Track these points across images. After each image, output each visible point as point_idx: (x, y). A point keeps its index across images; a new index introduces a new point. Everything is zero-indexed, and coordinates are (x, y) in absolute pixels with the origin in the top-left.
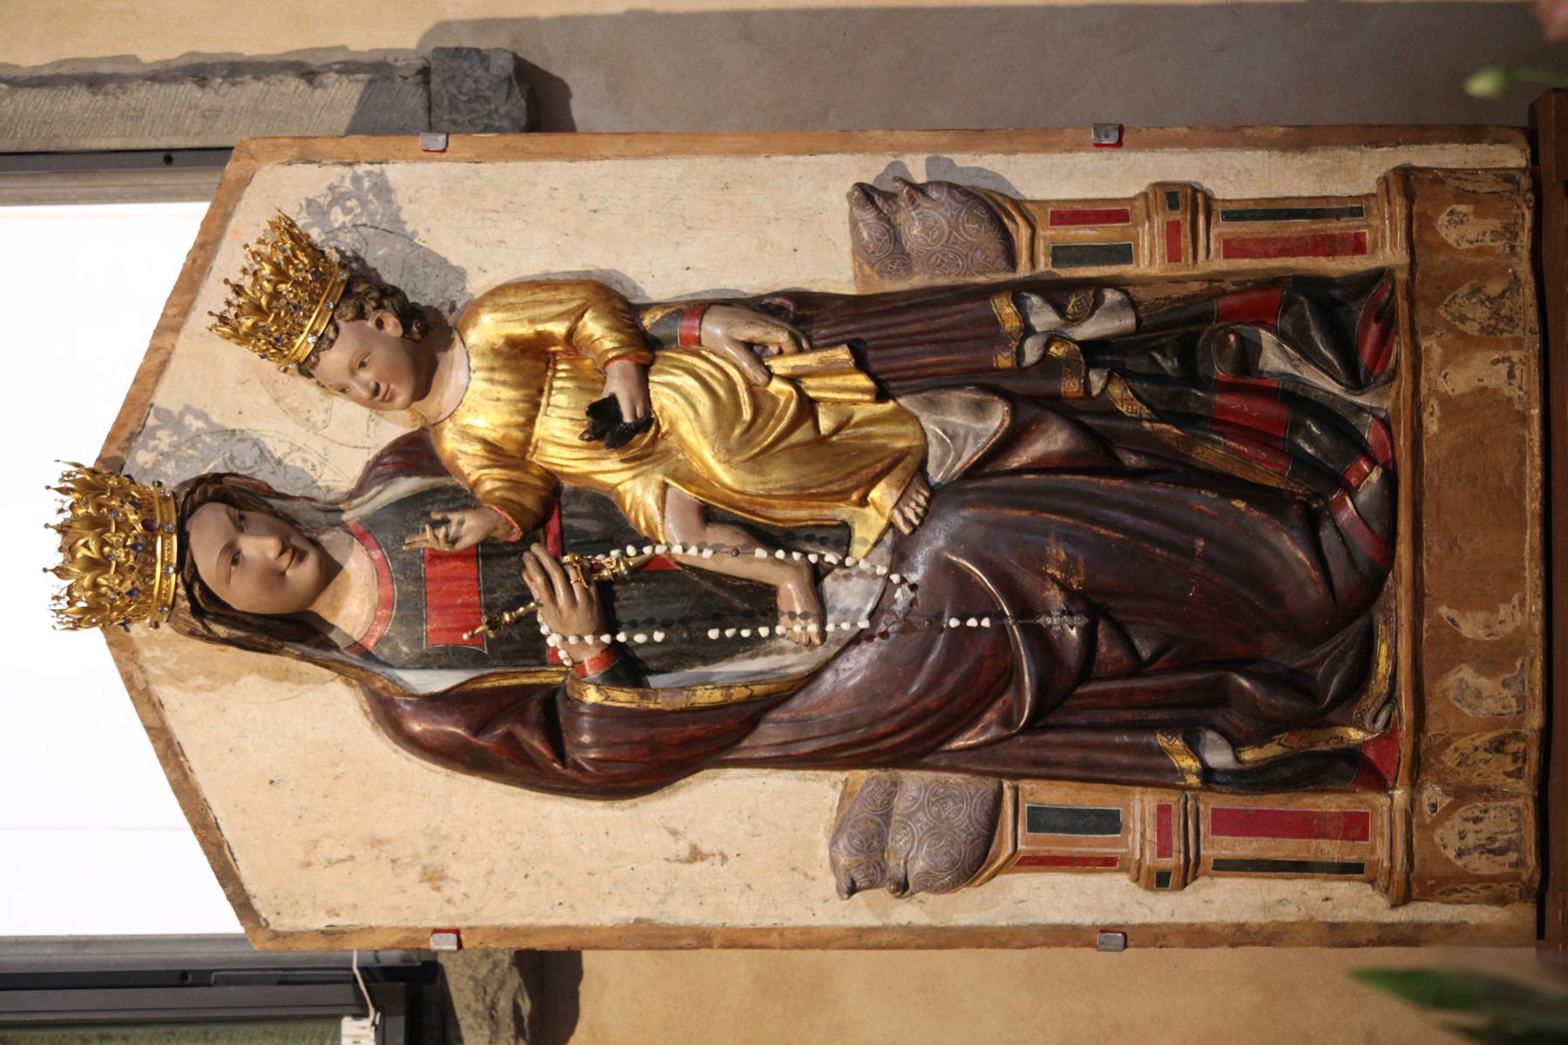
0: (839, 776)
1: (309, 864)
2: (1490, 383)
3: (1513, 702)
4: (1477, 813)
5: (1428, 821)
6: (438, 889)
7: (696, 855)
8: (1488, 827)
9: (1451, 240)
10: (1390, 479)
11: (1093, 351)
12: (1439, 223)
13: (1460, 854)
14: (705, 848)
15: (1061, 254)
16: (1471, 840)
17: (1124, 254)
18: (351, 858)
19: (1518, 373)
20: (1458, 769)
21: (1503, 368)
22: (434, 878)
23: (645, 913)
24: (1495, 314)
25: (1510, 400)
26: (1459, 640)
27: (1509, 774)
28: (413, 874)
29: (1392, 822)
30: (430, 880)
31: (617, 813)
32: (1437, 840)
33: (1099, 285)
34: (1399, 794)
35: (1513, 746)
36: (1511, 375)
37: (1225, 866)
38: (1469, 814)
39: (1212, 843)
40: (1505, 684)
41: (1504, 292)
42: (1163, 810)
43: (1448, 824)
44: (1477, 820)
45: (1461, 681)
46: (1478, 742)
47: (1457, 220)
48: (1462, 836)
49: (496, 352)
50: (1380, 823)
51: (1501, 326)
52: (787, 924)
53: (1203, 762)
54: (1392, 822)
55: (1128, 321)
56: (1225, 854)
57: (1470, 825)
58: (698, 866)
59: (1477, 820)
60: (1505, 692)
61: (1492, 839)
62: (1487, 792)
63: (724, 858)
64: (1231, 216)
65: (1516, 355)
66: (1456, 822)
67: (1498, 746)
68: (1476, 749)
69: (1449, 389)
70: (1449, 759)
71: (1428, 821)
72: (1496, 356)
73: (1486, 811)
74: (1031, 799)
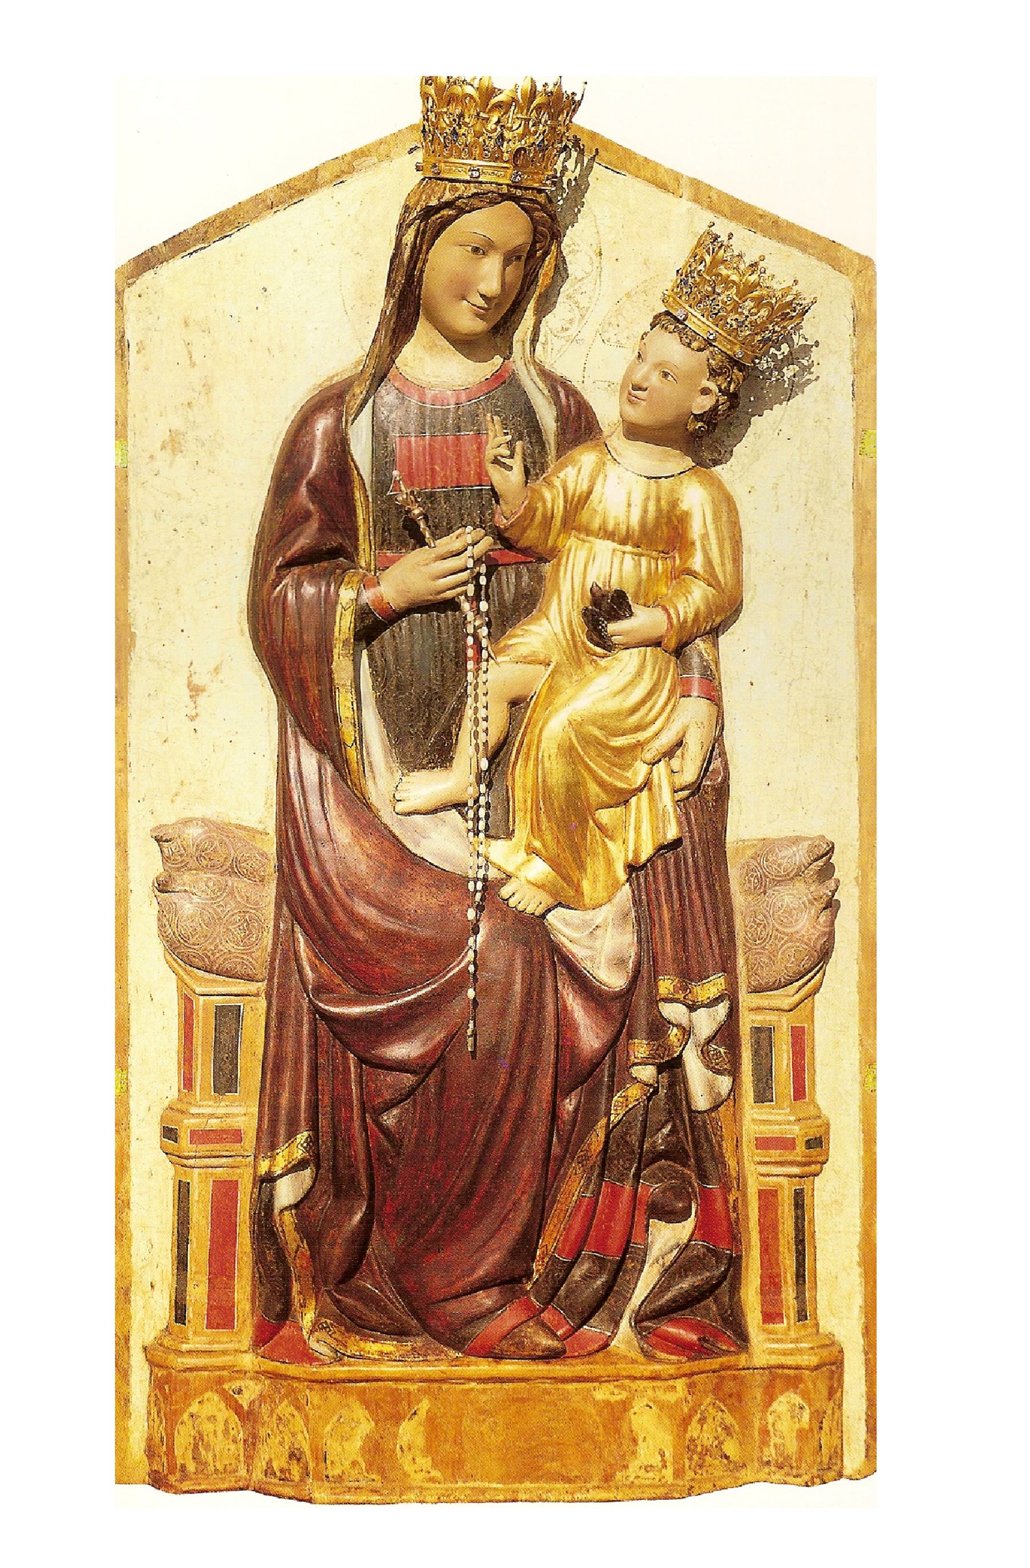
0: (271, 825)
1: (186, 324)
2: (642, 1449)
3: (337, 1472)
4: (232, 1433)
5: (226, 1386)
6: (163, 448)
7: (195, 691)
8: (219, 1443)
9: (775, 1405)
11: (671, 1067)
12: (792, 1395)
14: (202, 699)
15: (763, 1036)
16: (208, 1427)
17: (763, 1095)
18: (193, 365)
19: (651, 1475)
20: (275, 1416)
22: (174, 443)
23: (139, 642)
24: (706, 1451)
25: (626, 1467)
26: (397, 1419)
27: (269, 1463)
28: (177, 423)
29: (224, 1353)
30: (172, 440)
32: (208, 1394)
33: (734, 1072)
35: (296, 1471)
36: (648, 1468)
37: (183, 1191)
40: (354, 1463)
41: (727, 1457)
43: (223, 1405)
45: (358, 1422)
46: (300, 1437)
47: (796, 1412)
48: (212, 1418)
49: (674, 504)
50: (223, 1339)
51: (695, 1457)
52: (130, 777)
53: (281, 1176)
54: (224, 1353)
55: (701, 1102)
56: (194, 1195)
57: (221, 1427)
58: (187, 692)
59: (226, 1431)
60: (347, 1464)
61: (207, 1447)
62: (252, 1443)
63: (192, 719)
65: (668, 1473)
66: (224, 1413)
67: (294, 1456)
68: (293, 1435)
69: (636, 1409)
70: (285, 1408)
71: (226, 1386)
72: (667, 1454)
73: (235, 1441)
74: (248, 1009)
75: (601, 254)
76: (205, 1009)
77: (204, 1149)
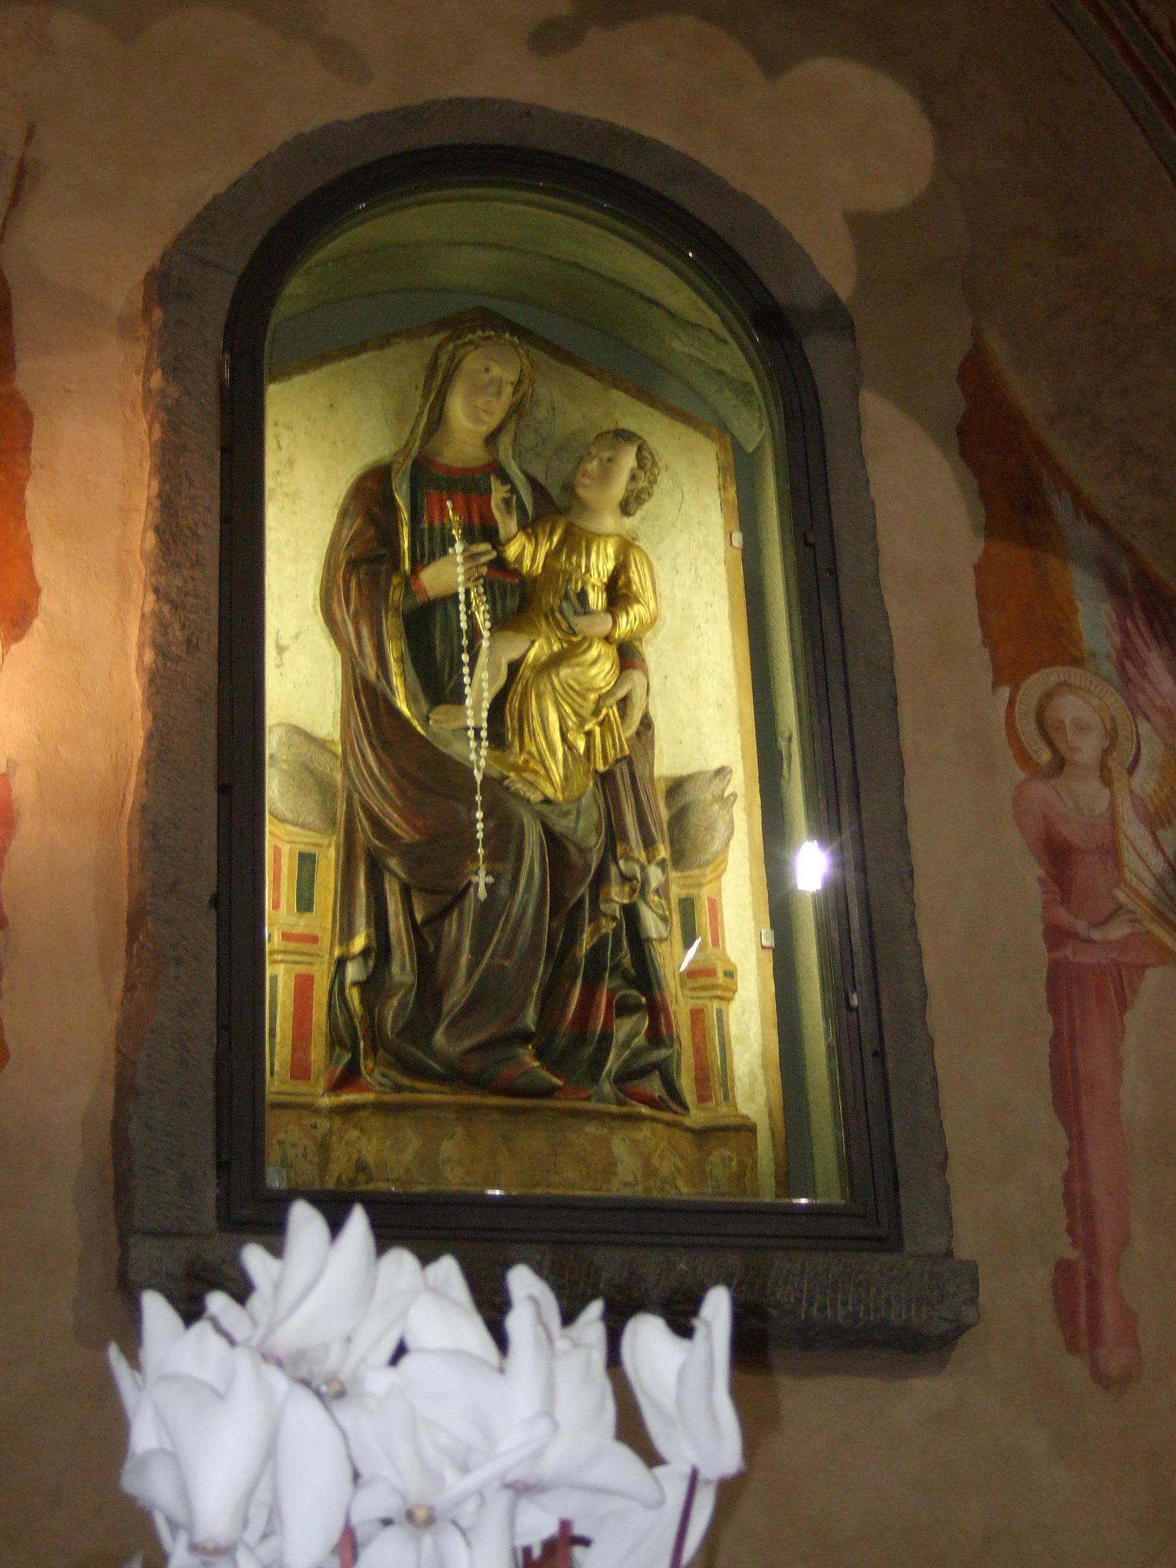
0: (337, 736)
4: (309, 1158)
10: (549, 1092)
12: (723, 1150)
13: (281, 1143)
14: (286, 655)
16: (291, 1152)
18: (280, 448)
20: (343, 1143)
21: (631, 1179)
29: (305, 1095)
31: (310, 602)
34: (326, 1101)
36: (626, 1184)
38: (309, 1151)
39: (287, 972)
40: (408, 1171)
42: (314, 939)
44: (305, 1156)
47: (726, 1161)
48: (294, 1145)
49: (343, 1125)
50: (302, 1087)
57: (300, 1151)
64: (720, 1013)
70: (353, 1134)
72: (638, 1173)
73: (311, 1162)
74: (321, 856)
75: (554, 408)
76: (291, 851)
77: (292, 946)
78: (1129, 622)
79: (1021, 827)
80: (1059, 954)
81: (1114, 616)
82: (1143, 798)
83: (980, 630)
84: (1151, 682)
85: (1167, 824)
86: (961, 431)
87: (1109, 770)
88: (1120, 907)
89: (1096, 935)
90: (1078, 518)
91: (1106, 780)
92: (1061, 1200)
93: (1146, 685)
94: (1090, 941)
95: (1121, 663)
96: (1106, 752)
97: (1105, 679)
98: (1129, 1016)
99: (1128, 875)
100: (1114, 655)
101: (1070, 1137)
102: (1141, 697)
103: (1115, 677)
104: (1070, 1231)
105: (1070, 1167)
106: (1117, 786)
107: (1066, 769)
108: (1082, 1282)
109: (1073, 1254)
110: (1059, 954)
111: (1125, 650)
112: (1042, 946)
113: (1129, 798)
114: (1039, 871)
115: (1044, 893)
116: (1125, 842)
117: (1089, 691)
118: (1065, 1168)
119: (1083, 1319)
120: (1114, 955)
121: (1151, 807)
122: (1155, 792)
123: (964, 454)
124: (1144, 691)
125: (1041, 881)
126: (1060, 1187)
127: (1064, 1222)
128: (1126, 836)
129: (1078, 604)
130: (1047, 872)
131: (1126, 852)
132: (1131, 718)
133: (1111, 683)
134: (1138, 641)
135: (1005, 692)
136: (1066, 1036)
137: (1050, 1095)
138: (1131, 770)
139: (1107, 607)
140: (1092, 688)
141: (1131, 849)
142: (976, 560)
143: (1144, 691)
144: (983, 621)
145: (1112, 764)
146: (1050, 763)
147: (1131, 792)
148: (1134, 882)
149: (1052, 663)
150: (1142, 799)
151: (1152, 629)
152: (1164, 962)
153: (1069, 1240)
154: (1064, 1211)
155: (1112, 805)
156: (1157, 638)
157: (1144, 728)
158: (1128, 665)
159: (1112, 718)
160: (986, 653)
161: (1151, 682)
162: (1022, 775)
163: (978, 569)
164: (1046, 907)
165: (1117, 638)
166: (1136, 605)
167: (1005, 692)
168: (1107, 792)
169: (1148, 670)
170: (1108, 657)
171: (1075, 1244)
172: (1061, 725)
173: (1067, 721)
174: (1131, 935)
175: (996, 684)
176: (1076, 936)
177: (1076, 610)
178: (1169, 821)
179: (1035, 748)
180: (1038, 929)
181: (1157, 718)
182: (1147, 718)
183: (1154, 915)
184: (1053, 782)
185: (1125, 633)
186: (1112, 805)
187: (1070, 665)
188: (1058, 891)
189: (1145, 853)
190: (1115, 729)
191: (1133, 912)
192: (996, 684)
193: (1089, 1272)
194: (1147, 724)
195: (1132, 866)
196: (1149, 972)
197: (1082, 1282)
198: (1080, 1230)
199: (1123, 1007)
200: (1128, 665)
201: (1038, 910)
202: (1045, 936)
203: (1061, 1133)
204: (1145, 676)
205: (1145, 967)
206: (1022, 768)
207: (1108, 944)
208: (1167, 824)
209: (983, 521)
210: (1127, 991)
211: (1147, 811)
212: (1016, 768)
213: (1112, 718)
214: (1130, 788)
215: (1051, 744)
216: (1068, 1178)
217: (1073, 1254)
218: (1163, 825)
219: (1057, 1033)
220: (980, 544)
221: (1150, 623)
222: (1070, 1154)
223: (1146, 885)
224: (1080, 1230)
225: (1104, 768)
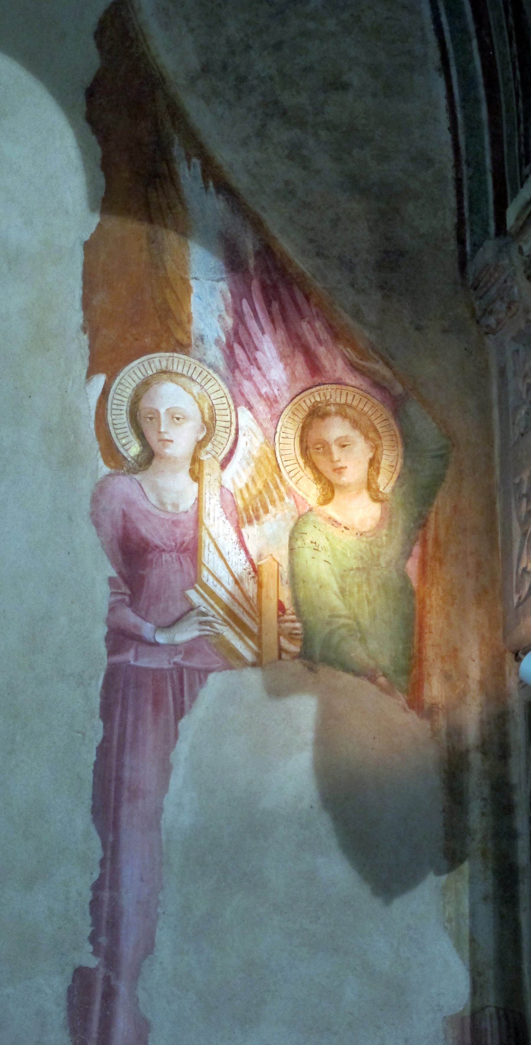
78: (245, 302)
79: (97, 525)
80: (117, 659)
81: (229, 295)
82: (233, 491)
83: (81, 314)
84: (259, 368)
85: (255, 521)
86: (90, 94)
87: (200, 462)
88: (192, 609)
89: (161, 638)
90: (206, 188)
91: (196, 476)
92: (87, 907)
93: (254, 371)
94: (157, 644)
95: (230, 347)
96: (200, 444)
97: (210, 366)
98: (183, 722)
99: (205, 573)
100: (224, 339)
101: (104, 846)
102: (247, 386)
103: (221, 364)
104: (93, 939)
105: (102, 876)
106: (206, 479)
107: (155, 462)
108: (99, 989)
109: (92, 962)
110: (117, 659)
111: (236, 333)
112: (103, 650)
113: (218, 492)
114: (112, 572)
115: (113, 594)
116: (206, 540)
117: (191, 379)
118: (96, 876)
119: (94, 1026)
120: (178, 659)
121: (240, 503)
122: (247, 486)
123: (90, 119)
124: (250, 378)
125: (111, 581)
126: (88, 896)
127: (88, 930)
128: (209, 534)
129: (193, 283)
130: (119, 573)
131: (206, 548)
132: (232, 407)
133: (216, 370)
134: (252, 324)
135: (100, 380)
136: (115, 743)
137: (89, 802)
138: (224, 465)
139: (223, 286)
140: (194, 377)
141: (212, 547)
142: (87, 237)
143: (250, 378)
144: (86, 304)
145: (204, 457)
146: (138, 456)
147: (222, 486)
148: (211, 582)
149: (157, 349)
150: (232, 494)
151: (270, 313)
152: (231, 668)
153: (90, 948)
154: (89, 919)
155: (199, 500)
156: (273, 321)
157: (245, 417)
158: (238, 350)
159: (212, 407)
160: (85, 339)
161: (259, 368)
162: (105, 470)
163: (88, 246)
164: (112, 609)
165: (230, 321)
166: (255, 284)
167: (100, 380)
168: (196, 485)
169: (259, 355)
170: (217, 342)
171: (96, 953)
172: (155, 416)
173: (162, 411)
174: (200, 637)
175: (91, 372)
176: (139, 639)
177: (189, 289)
178: (258, 518)
179: (124, 441)
180: (101, 631)
181: (261, 407)
182: (251, 408)
183: (226, 617)
184: (138, 477)
185: (239, 315)
186: (199, 500)
187: (174, 351)
188: (128, 592)
189: (227, 551)
190: (213, 418)
191: (204, 614)
192: (91, 372)
193: (107, 979)
194: (248, 413)
195: (210, 566)
196: (211, 677)
197: (99, 989)
198: (103, 940)
199: (180, 712)
200: (238, 350)
201: (103, 609)
202: (107, 639)
203: (96, 842)
204: (254, 361)
205: (208, 671)
206: (107, 462)
207: (173, 648)
208: (255, 521)
209: (102, 193)
210: (186, 698)
211: (236, 507)
212: (101, 462)
213: (212, 407)
214: (220, 482)
215: (141, 436)
216: (97, 887)
217: (92, 962)
218: (250, 522)
219: (106, 739)
220: (96, 219)
221: (268, 303)
222: (102, 863)
223: (222, 585)
224: (103, 940)
225: (195, 460)
